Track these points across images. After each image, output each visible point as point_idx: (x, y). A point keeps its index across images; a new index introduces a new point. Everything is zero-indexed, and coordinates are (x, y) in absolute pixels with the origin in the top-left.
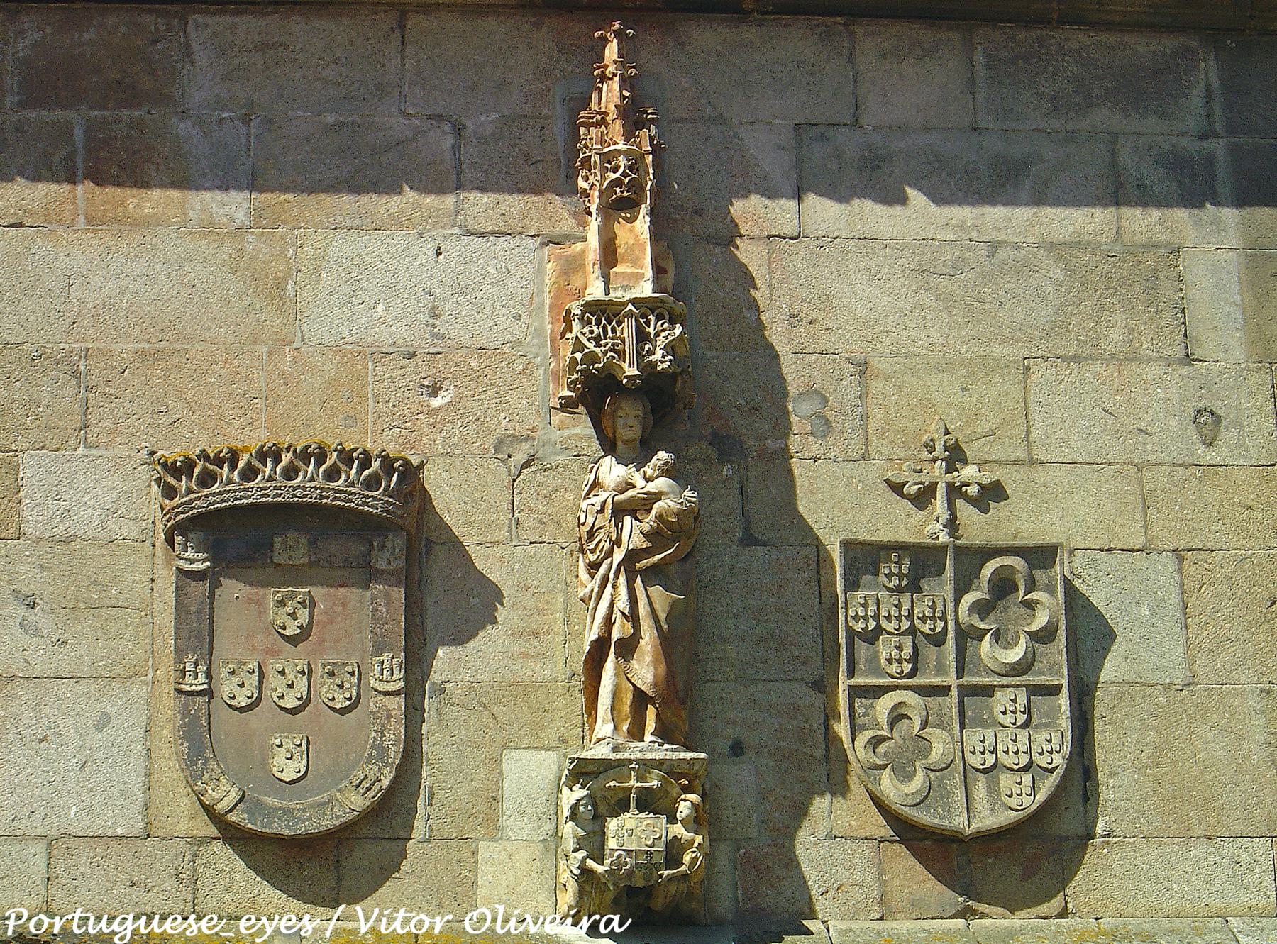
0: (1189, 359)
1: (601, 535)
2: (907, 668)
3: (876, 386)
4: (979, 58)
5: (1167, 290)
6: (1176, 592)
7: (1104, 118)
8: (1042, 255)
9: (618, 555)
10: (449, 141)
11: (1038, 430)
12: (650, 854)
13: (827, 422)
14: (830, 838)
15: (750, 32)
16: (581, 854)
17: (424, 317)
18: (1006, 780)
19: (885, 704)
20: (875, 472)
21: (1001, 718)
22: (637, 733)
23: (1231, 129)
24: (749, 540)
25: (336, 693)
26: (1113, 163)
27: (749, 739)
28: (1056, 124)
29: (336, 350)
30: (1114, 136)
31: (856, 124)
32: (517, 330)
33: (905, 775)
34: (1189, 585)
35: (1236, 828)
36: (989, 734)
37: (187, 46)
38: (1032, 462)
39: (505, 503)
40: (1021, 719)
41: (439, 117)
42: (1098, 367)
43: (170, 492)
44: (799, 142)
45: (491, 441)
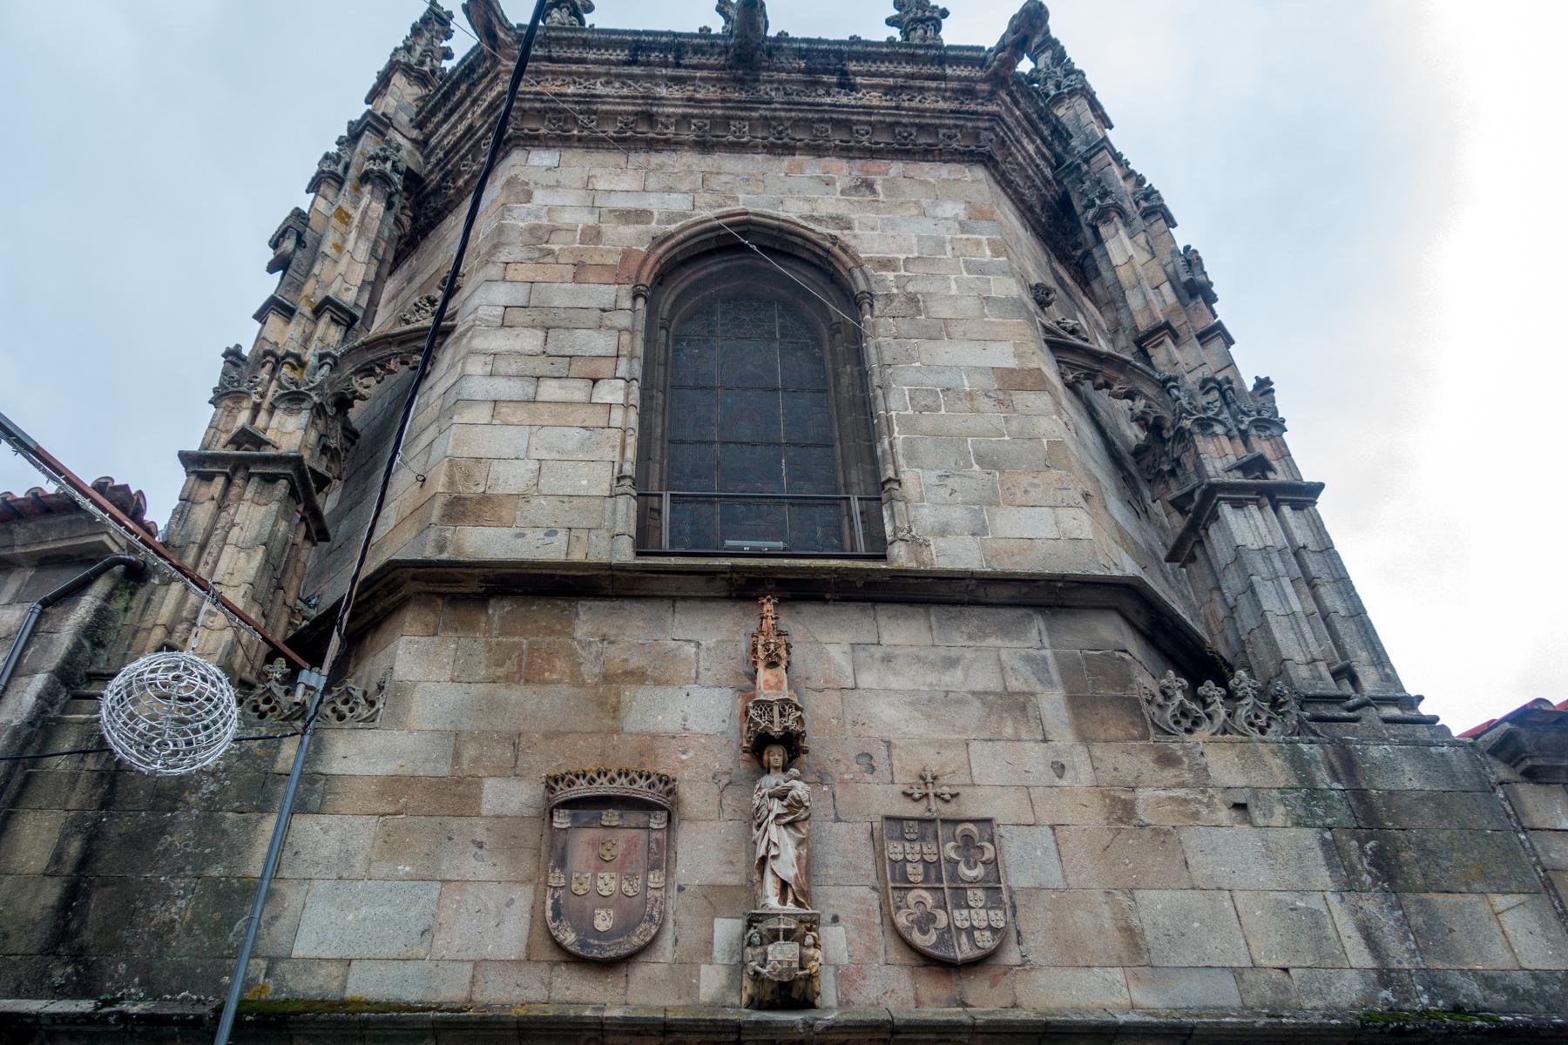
0: (1045, 740)
1: (763, 808)
2: (920, 878)
3: (895, 752)
4: (933, 619)
5: (1030, 711)
6: (1053, 845)
7: (992, 641)
8: (970, 696)
9: (771, 817)
10: (694, 650)
11: (975, 771)
12: (790, 963)
13: (873, 767)
14: (886, 964)
15: (829, 608)
16: (753, 964)
17: (681, 721)
18: (977, 934)
19: (912, 896)
20: (898, 788)
21: (971, 904)
22: (783, 901)
23: (1052, 646)
24: (837, 820)
25: (629, 888)
26: (999, 660)
27: (841, 914)
28: (971, 644)
29: (638, 734)
30: (999, 648)
31: (879, 644)
32: (724, 727)
33: (924, 932)
34: (1060, 841)
35: (1103, 961)
36: (965, 912)
37: (577, 614)
38: (974, 785)
39: (717, 802)
40: (981, 904)
41: (689, 641)
42: (1001, 743)
43: (551, 789)
44: (853, 651)
45: (710, 775)
